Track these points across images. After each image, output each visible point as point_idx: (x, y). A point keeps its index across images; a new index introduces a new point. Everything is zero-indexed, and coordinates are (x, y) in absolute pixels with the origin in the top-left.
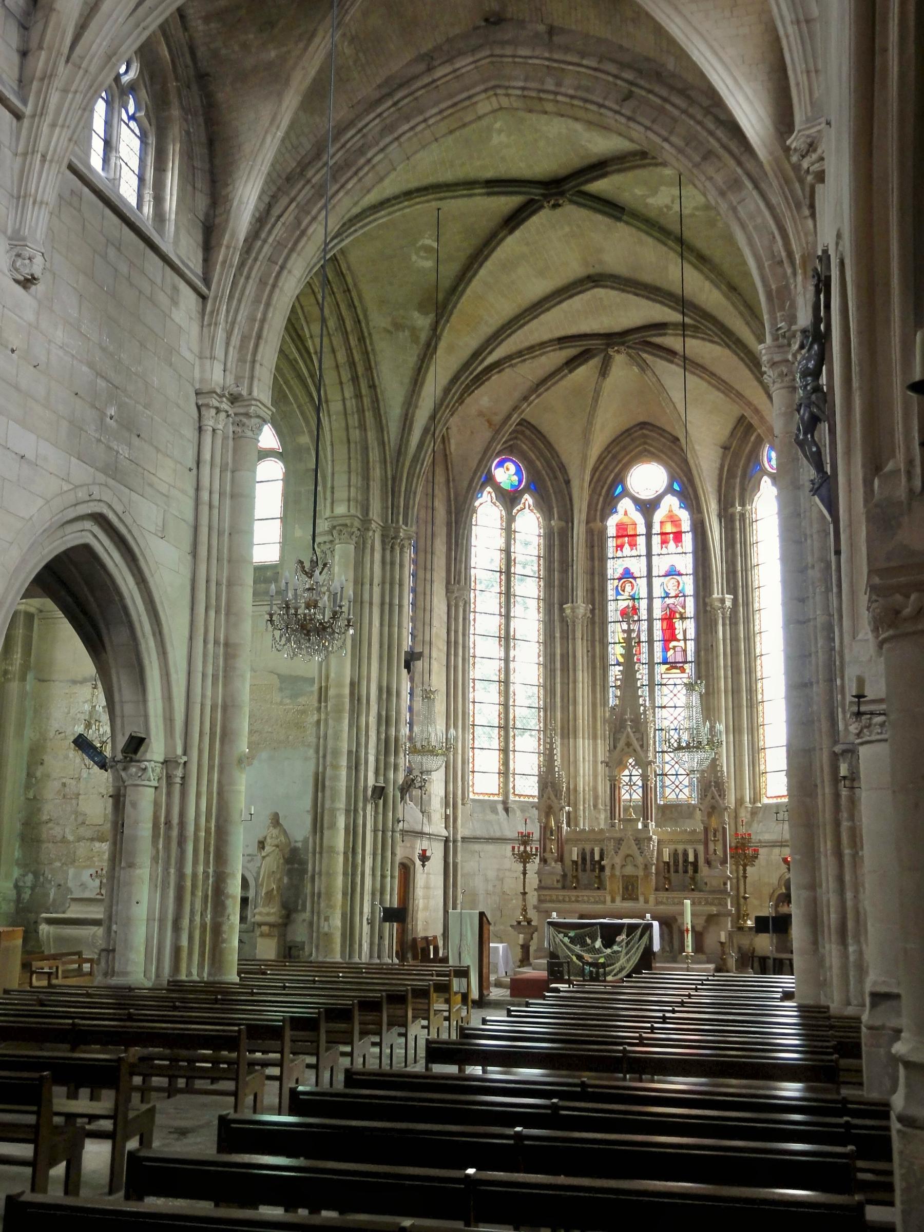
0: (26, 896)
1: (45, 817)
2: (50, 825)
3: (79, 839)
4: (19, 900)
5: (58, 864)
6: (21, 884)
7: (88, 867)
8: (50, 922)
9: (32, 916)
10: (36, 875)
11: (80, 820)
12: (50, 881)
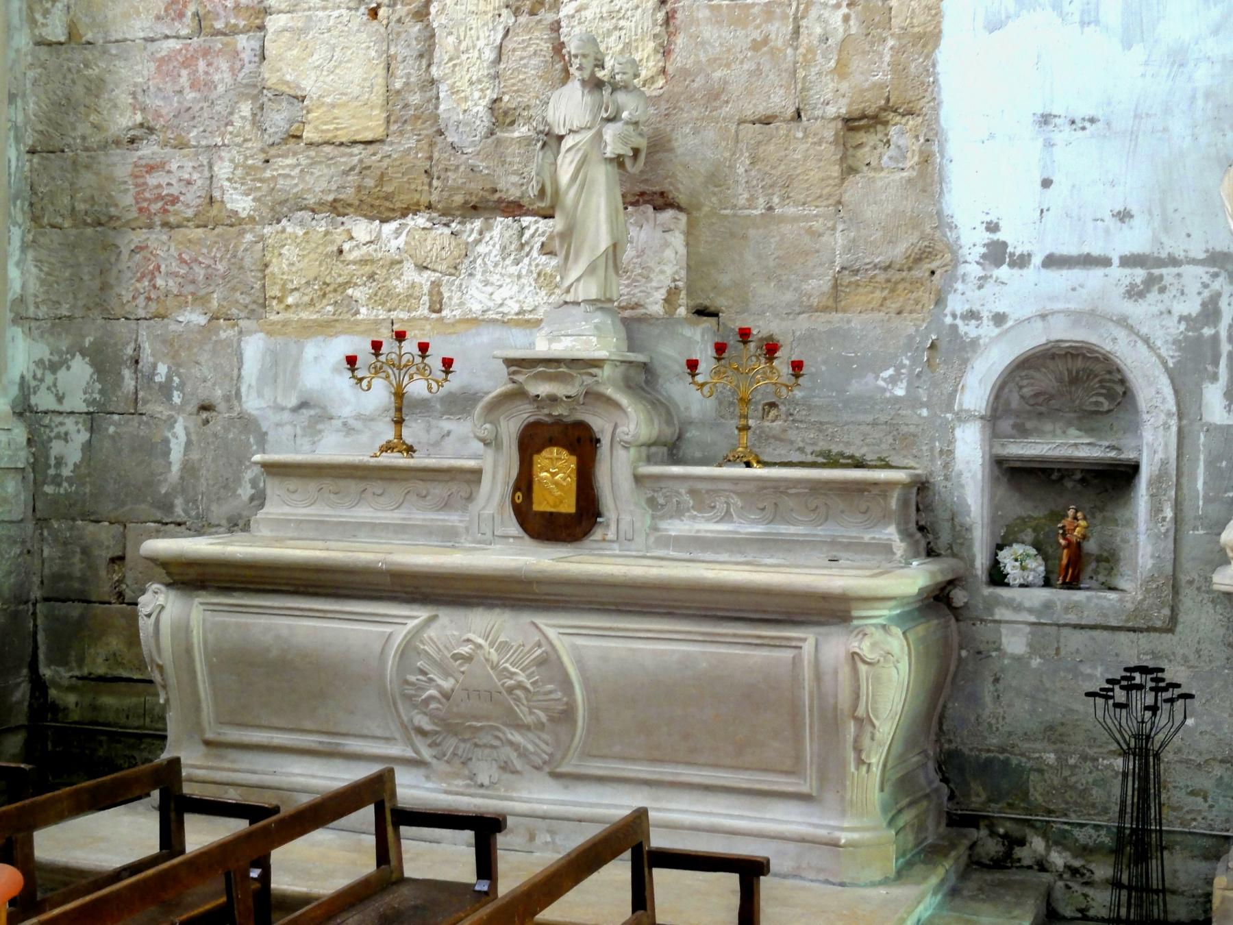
0: (70, 449)
1: (124, 121)
2: (148, 150)
3: (281, 208)
4: (39, 466)
5: (197, 318)
6: (43, 400)
7: (326, 328)
8: (193, 577)
9: (103, 536)
10: (105, 363)
11: (278, 119)
12: (166, 390)
